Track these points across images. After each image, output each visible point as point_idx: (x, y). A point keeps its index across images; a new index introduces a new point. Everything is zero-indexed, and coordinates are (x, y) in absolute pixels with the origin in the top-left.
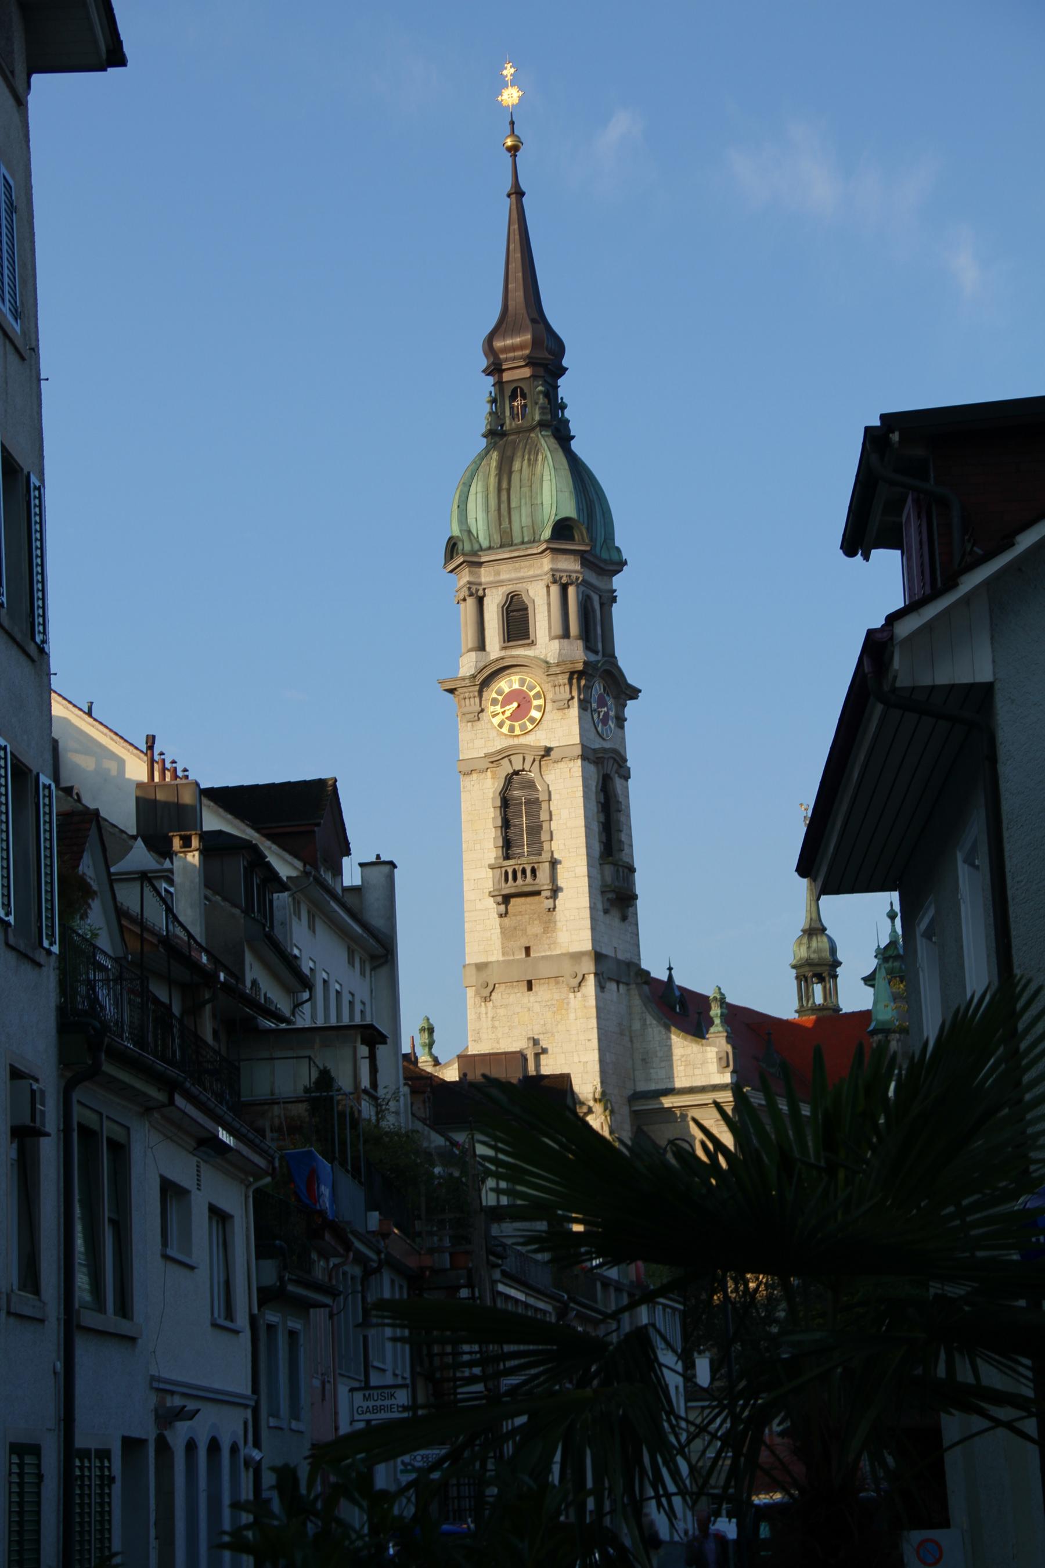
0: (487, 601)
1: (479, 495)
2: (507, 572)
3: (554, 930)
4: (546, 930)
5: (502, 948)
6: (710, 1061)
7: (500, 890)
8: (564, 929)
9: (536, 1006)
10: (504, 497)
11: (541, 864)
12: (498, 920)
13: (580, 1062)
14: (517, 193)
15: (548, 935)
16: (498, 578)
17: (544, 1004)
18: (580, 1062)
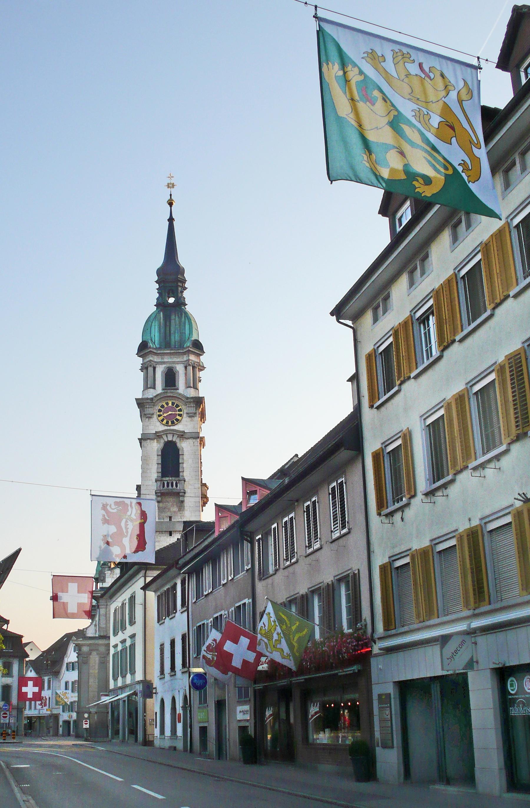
0: (157, 369)
1: (156, 327)
2: (166, 359)
3: (183, 510)
4: (180, 510)
7: (160, 490)
8: (188, 510)
10: (168, 329)
14: (171, 220)
15: (181, 512)
16: (162, 361)
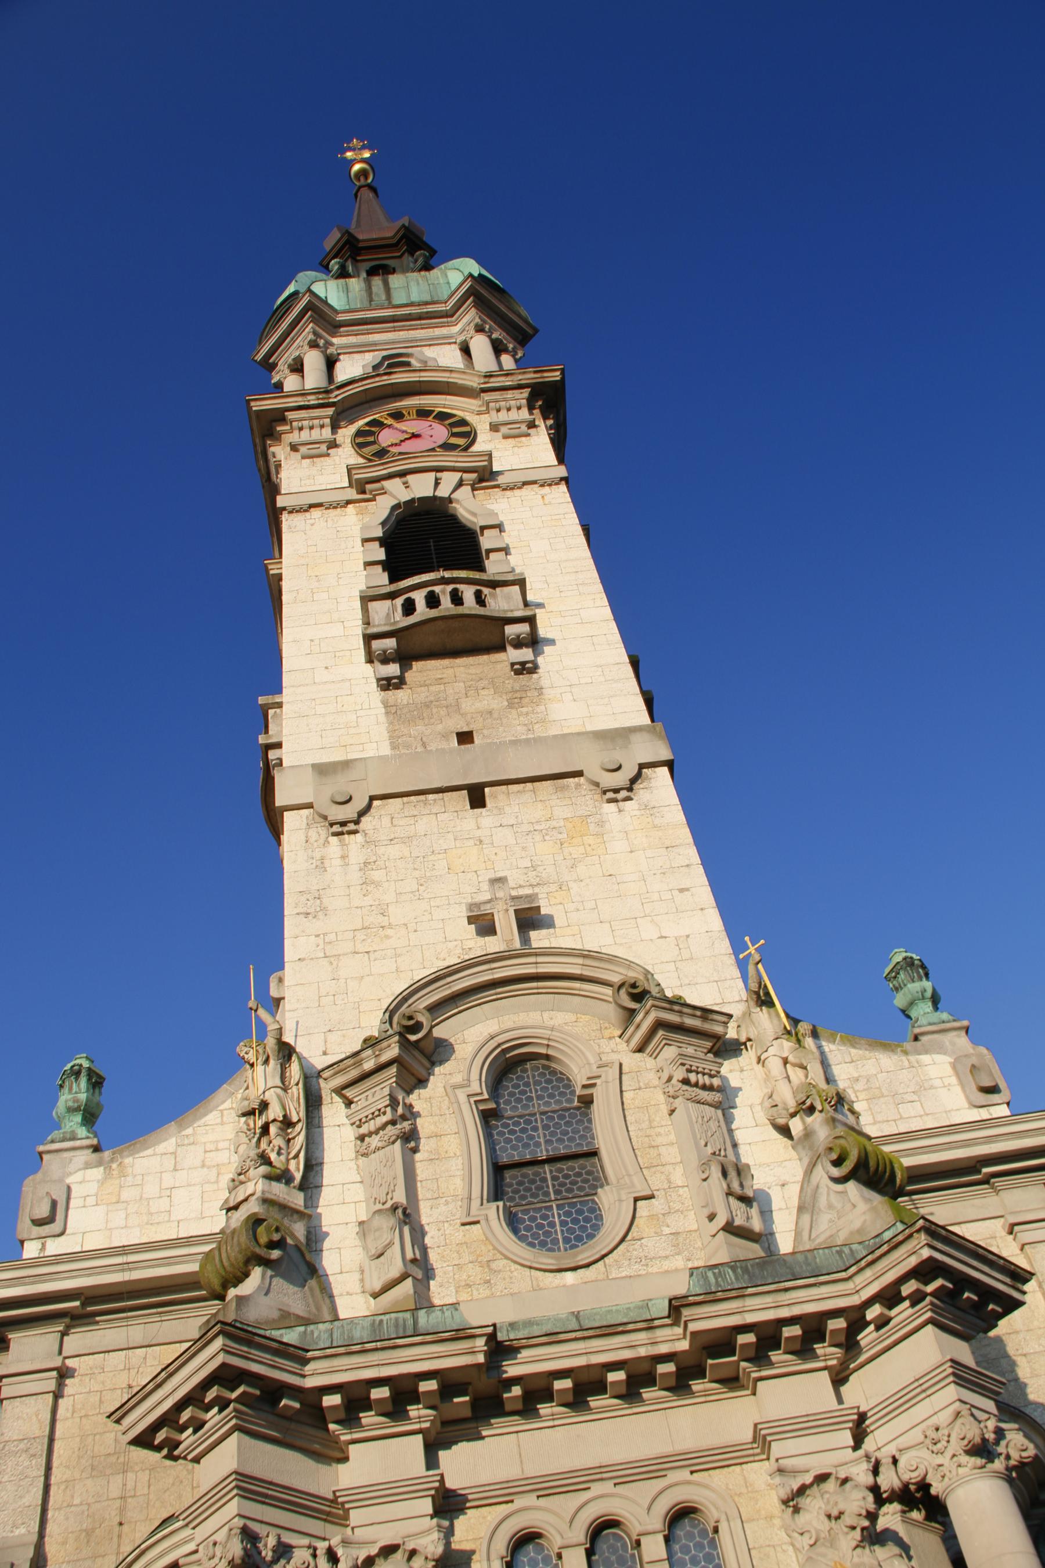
4: (515, 701)
5: (391, 737)
6: (937, 1083)
9: (504, 836)
11: (498, 590)
12: (377, 696)
13: (662, 937)
15: (524, 710)
17: (526, 827)
18: (662, 937)
